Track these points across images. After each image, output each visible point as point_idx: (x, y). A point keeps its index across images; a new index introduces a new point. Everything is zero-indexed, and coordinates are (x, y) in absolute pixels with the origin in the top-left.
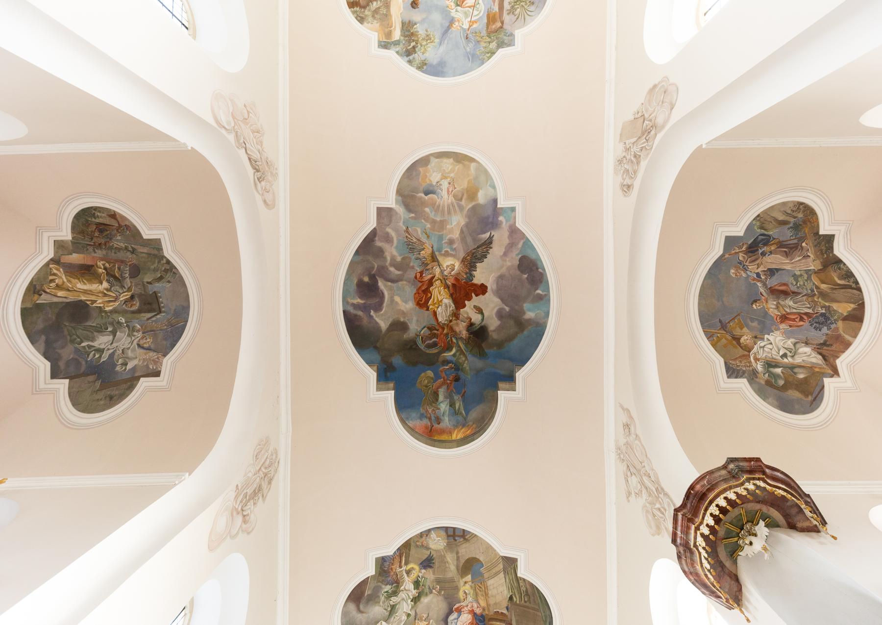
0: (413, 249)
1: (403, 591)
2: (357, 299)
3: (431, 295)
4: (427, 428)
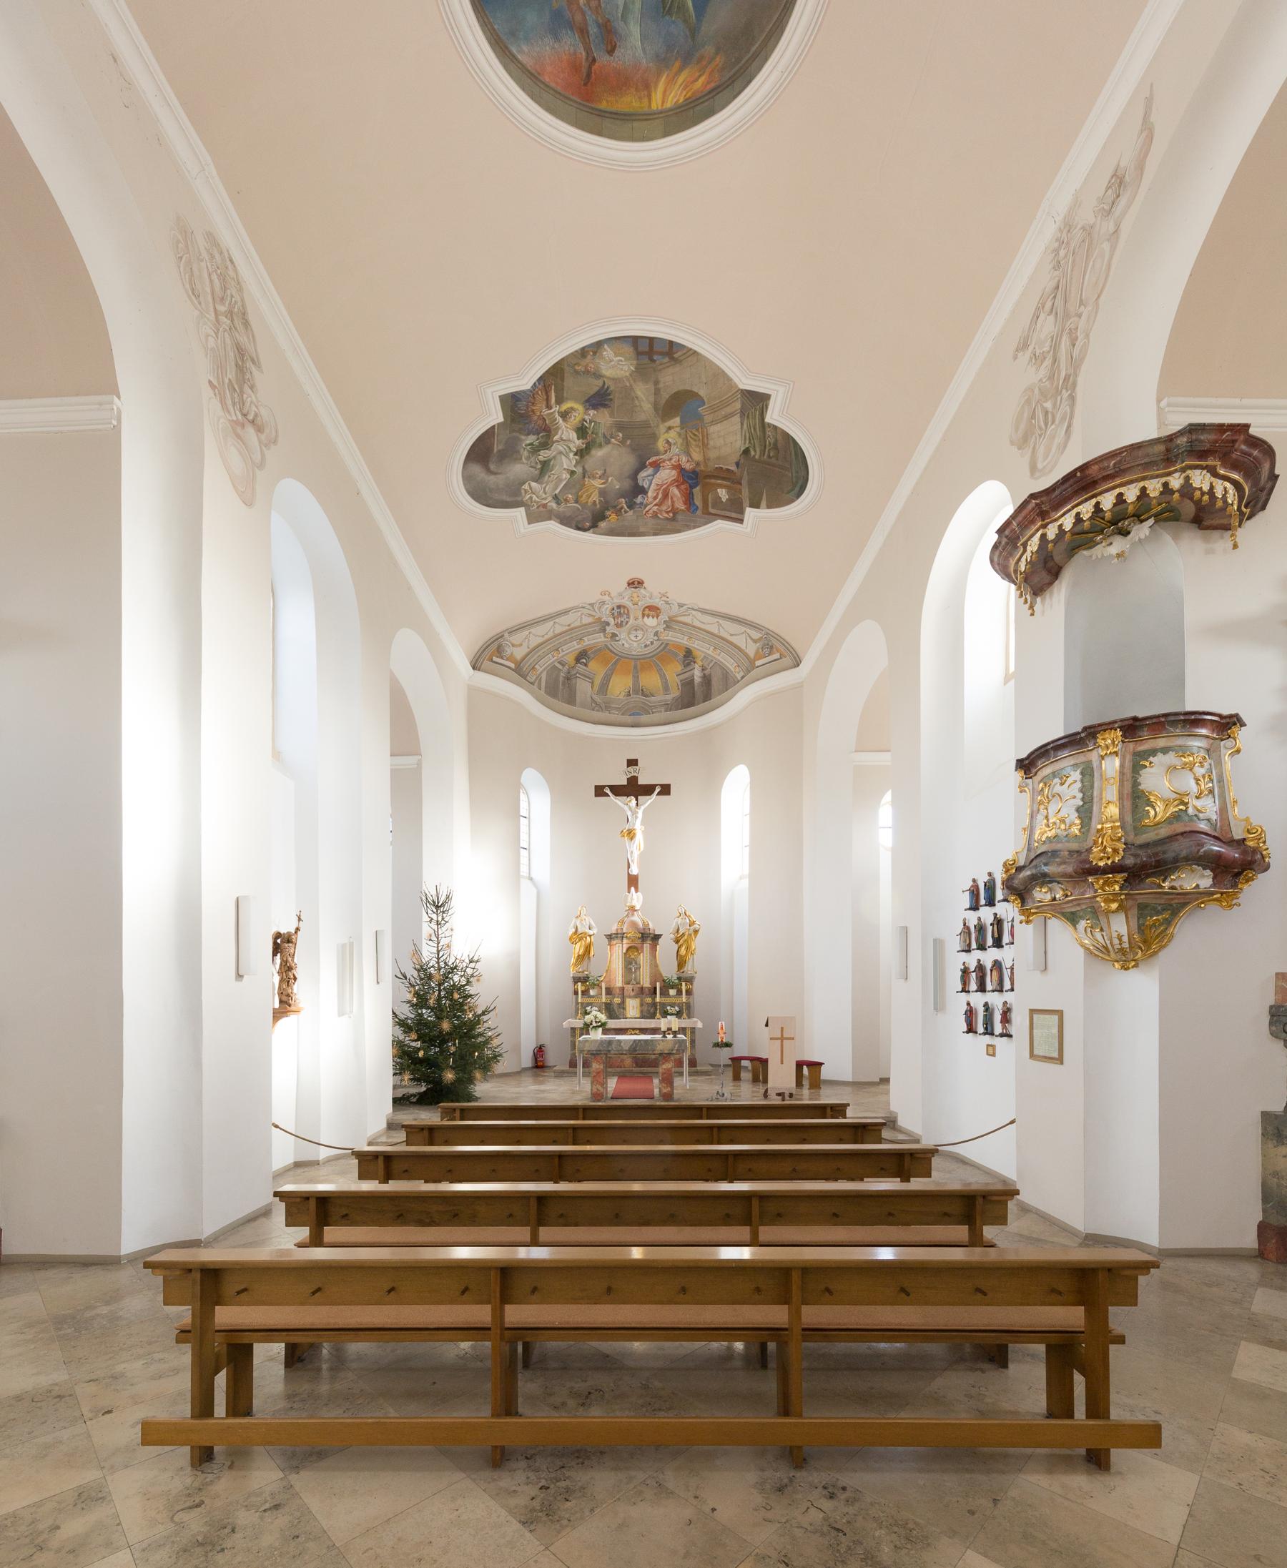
1: (558, 441)
4: (575, 67)
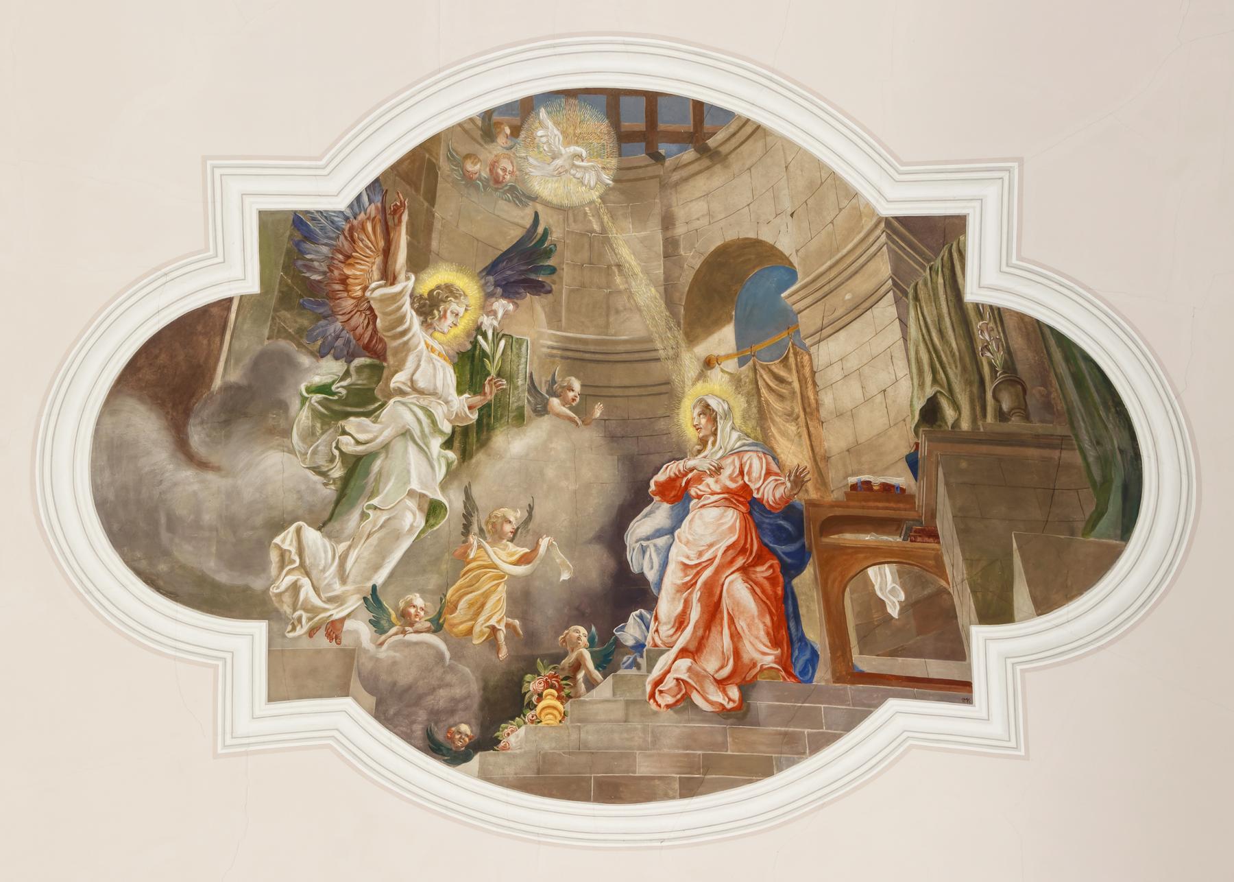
1: (401, 393)
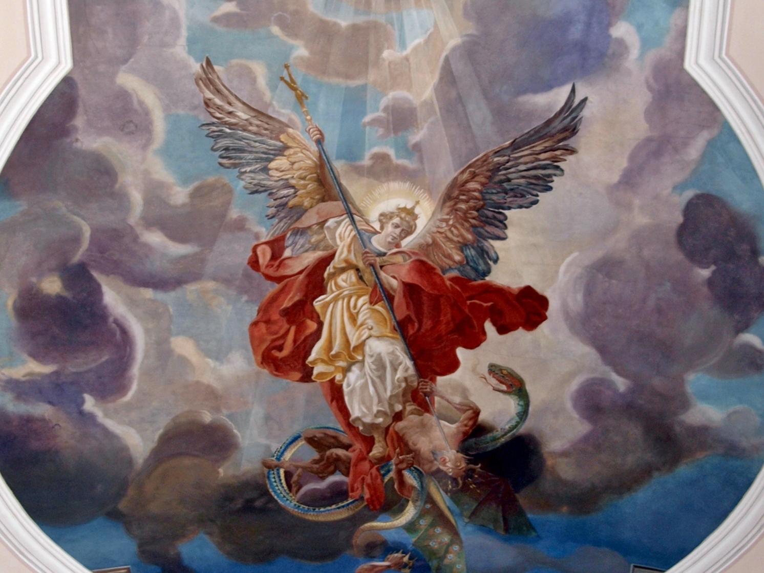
0: (241, 150)
2: (24, 362)
3: (321, 324)
